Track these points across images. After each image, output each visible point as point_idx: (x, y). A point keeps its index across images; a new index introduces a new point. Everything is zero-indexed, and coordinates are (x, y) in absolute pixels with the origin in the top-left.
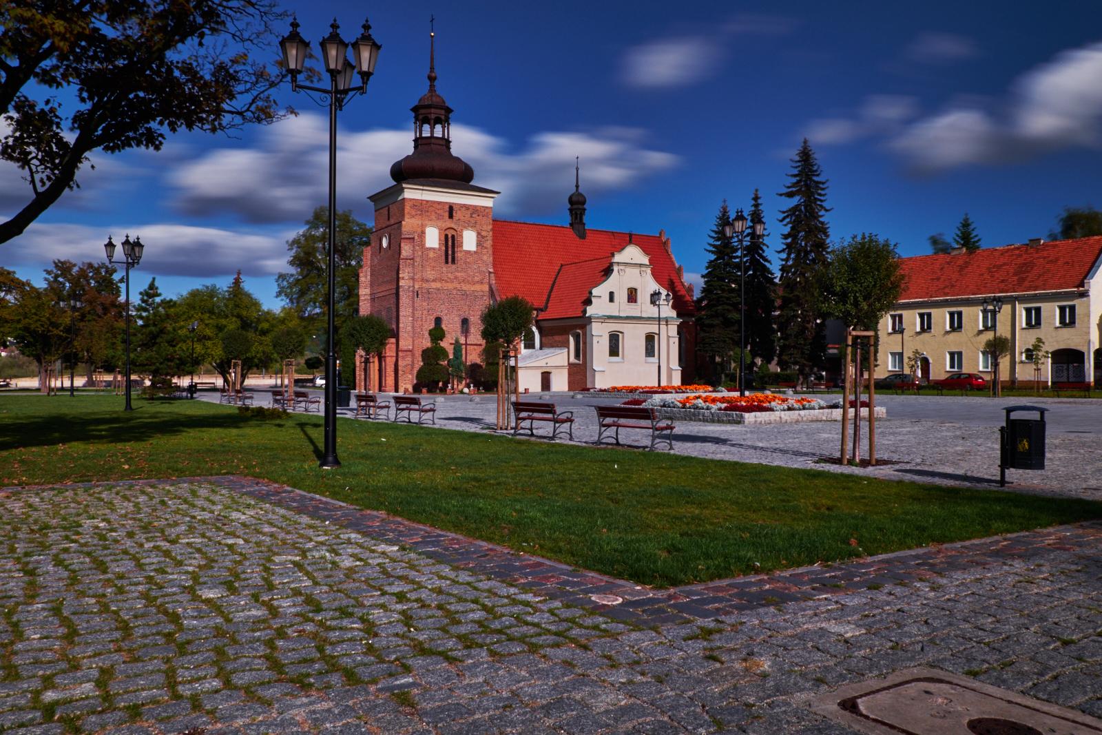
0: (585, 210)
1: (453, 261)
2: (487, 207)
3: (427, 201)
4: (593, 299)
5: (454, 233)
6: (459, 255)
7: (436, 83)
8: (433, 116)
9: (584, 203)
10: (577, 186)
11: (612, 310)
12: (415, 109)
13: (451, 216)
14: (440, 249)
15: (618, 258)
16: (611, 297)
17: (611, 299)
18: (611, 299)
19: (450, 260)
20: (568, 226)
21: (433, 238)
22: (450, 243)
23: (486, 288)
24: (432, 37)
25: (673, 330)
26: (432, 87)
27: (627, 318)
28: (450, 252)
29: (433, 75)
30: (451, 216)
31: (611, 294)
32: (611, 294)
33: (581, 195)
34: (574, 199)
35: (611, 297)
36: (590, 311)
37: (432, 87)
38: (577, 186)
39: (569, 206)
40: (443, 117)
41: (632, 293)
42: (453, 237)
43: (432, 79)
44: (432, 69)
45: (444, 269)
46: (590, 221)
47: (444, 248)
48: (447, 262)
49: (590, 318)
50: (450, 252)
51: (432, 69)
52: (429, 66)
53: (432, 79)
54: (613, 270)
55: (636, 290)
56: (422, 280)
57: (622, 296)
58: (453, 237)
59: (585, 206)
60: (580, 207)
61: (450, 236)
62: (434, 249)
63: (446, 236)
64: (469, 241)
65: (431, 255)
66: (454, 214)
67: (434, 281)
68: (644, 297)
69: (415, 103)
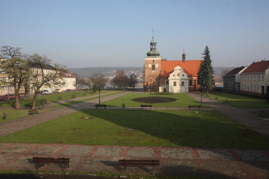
1: (154, 70)
6: (155, 68)
7: (154, 39)
11: (174, 78)
12: (151, 43)
13: (153, 62)
14: (151, 68)
15: (175, 68)
16: (174, 75)
21: (150, 66)
25: (187, 81)
27: (177, 79)
30: (153, 62)
35: (174, 75)
36: (169, 78)
42: (154, 65)
46: (187, 59)
48: (153, 70)
53: (153, 38)
57: (176, 75)
64: (157, 66)
69: (150, 42)
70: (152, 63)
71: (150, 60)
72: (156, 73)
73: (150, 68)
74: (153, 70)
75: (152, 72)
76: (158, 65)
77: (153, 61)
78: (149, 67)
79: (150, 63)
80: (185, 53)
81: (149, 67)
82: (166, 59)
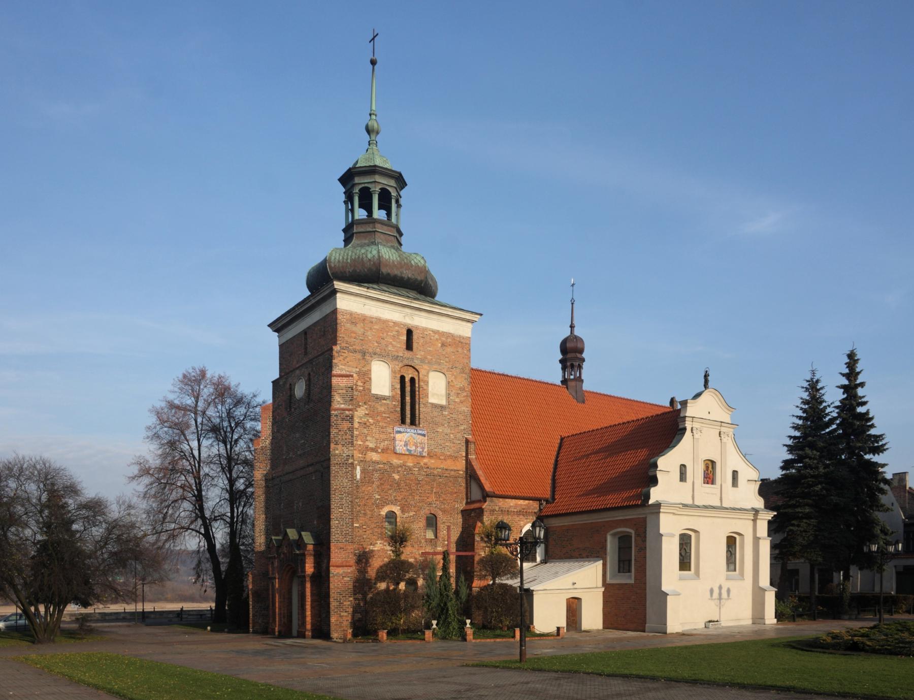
0: (583, 360)
4: (660, 476)
5: (415, 375)
9: (581, 351)
10: (572, 327)
13: (409, 346)
17: (683, 477)
18: (683, 477)
19: (408, 420)
20: (561, 384)
22: (408, 389)
23: (461, 465)
25: (763, 528)
30: (409, 346)
31: (683, 468)
32: (683, 468)
33: (576, 337)
36: (656, 494)
38: (572, 327)
41: (707, 468)
42: (412, 380)
48: (403, 422)
49: (658, 505)
54: (685, 429)
55: (713, 462)
57: (696, 472)
58: (412, 380)
59: (583, 355)
60: (578, 355)
61: (407, 379)
62: (385, 398)
63: (402, 378)
66: (415, 345)
68: (723, 475)
70: (396, 358)
71: (384, 324)
72: (430, 455)
73: (379, 398)
74: (403, 422)
75: (400, 448)
76: (449, 384)
78: (375, 390)
79: (383, 356)
80: (577, 332)
81: (375, 390)
82: (273, 382)
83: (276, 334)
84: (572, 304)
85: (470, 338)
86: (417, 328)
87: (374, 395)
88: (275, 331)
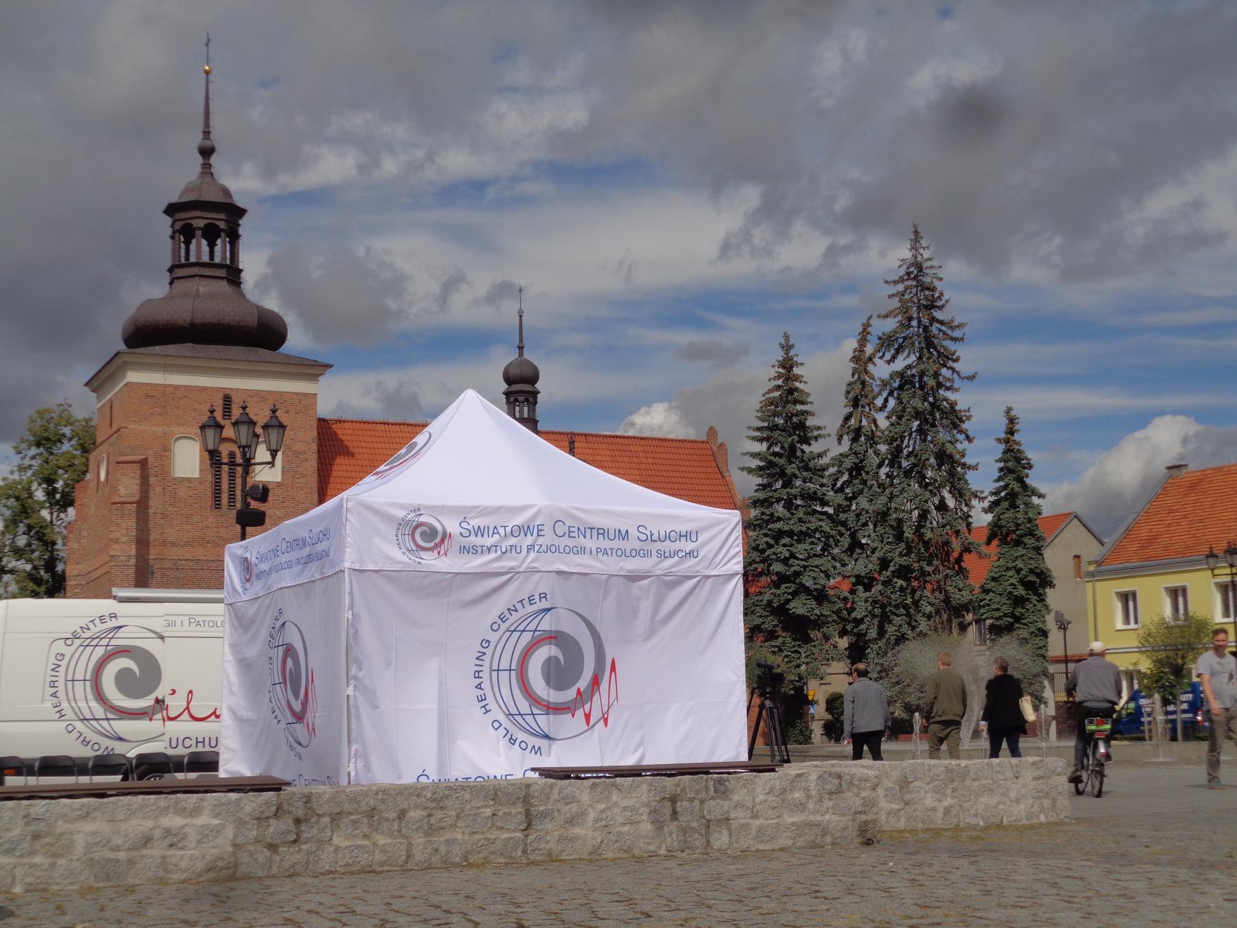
2: (306, 395)
3: (176, 387)
7: (214, 160)
8: (200, 223)
14: (200, 481)
24: (207, 73)
26: (207, 167)
28: (225, 486)
29: (208, 143)
34: (515, 372)
37: (207, 167)
39: (505, 386)
40: (222, 225)
43: (206, 152)
44: (207, 133)
45: (211, 519)
47: (209, 478)
50: (225, 486)
51: (207, 133)
52: (201, 128)
53: (206, 152)
56: (164, 543)
62: (189, 480)
65: (183, 492)
67: (189, 543)
77: (227, 400)
83: (95, 395)
84: (521, 316)
85: (316, 394)
86: (237, 390)
87: (175, 479)
88: (93, 391)
